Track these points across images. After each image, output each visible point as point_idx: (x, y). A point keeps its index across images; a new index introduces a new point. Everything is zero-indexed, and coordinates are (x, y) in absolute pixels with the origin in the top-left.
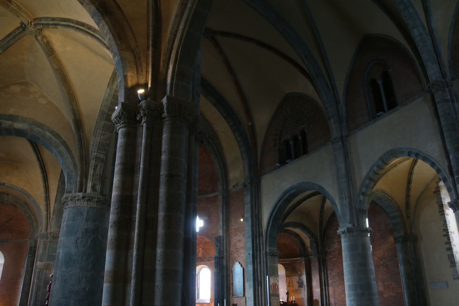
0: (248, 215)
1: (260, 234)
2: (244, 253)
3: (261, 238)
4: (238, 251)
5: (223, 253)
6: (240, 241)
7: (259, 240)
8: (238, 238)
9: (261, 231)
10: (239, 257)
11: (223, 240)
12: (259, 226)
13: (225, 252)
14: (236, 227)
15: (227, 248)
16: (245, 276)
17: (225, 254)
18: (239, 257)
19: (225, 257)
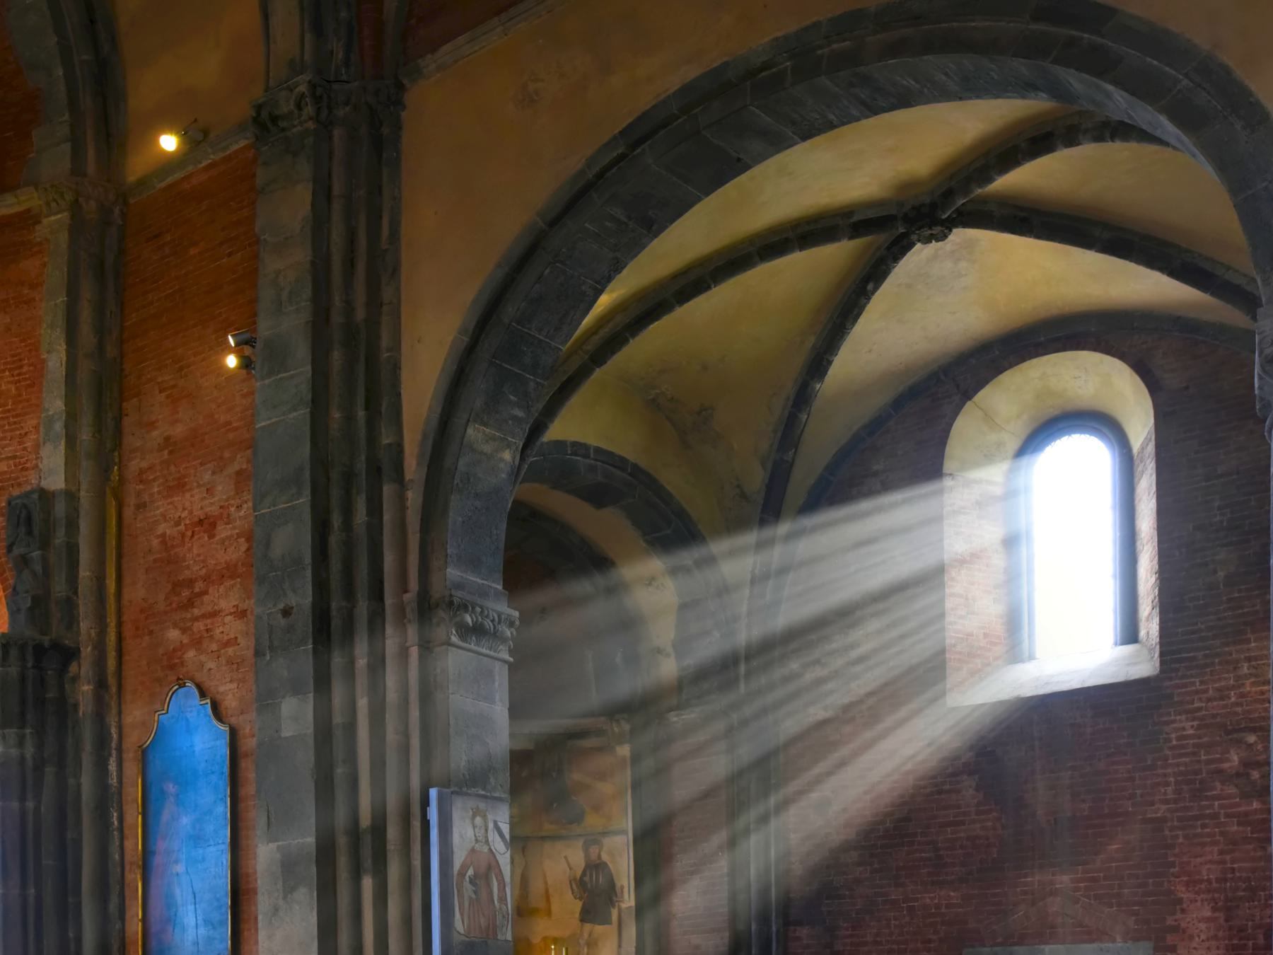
0: (288, 324)
1: (384, 467)
2: (241, 614)
3: (388, 490)
4: (190, 604)
5: (71, 620)
6: (207, 524)
7: (375, 509)
8: (194, 503)
9: (386, 439)
10: (197, 643)
11: (72, 524)
12: (371, 405)
13: (85, 606)
14: (179, 430)
15: (100, 580)
16: (249, 789)
17: (86, 626)
18: (197, 643)
19: (87, 651)
